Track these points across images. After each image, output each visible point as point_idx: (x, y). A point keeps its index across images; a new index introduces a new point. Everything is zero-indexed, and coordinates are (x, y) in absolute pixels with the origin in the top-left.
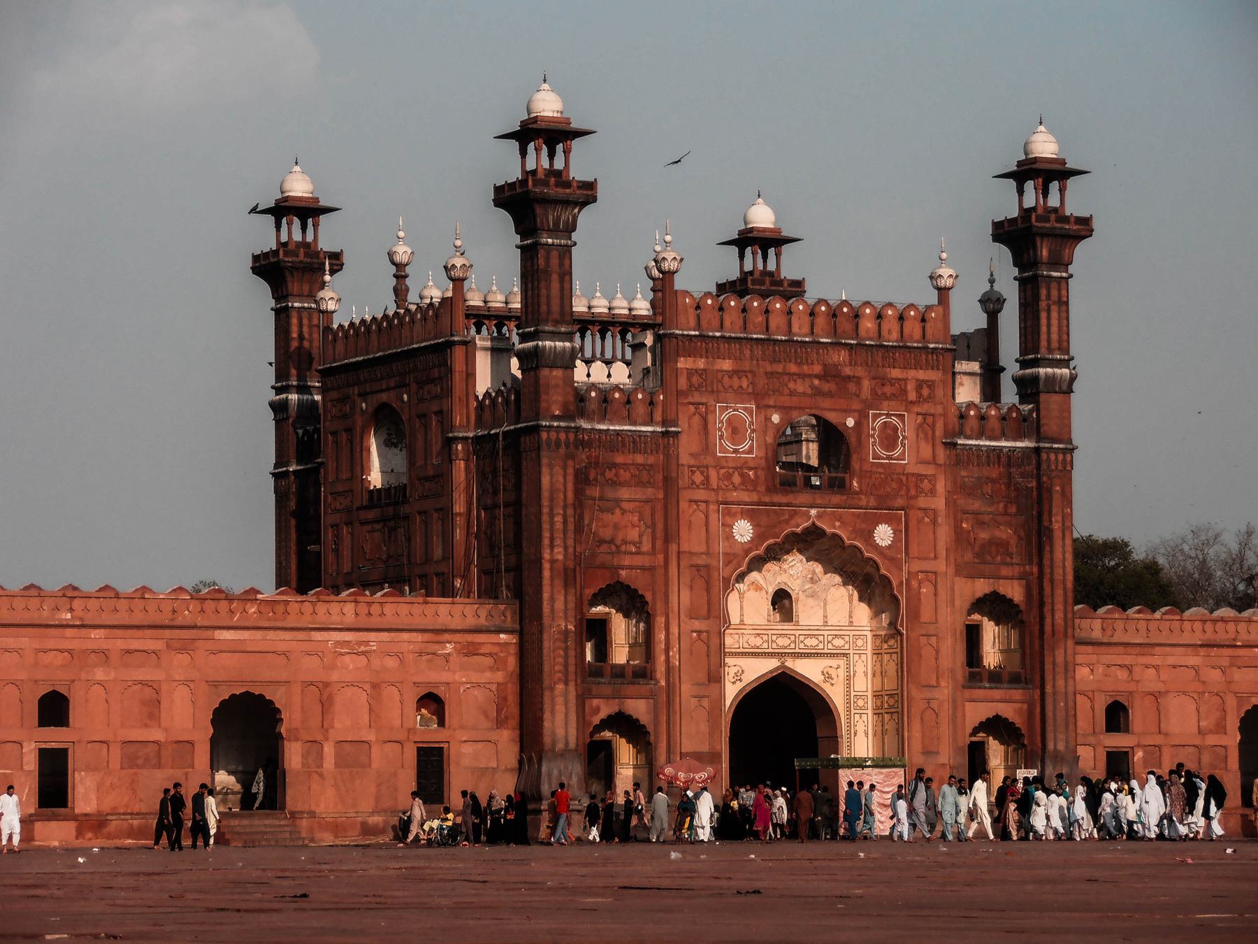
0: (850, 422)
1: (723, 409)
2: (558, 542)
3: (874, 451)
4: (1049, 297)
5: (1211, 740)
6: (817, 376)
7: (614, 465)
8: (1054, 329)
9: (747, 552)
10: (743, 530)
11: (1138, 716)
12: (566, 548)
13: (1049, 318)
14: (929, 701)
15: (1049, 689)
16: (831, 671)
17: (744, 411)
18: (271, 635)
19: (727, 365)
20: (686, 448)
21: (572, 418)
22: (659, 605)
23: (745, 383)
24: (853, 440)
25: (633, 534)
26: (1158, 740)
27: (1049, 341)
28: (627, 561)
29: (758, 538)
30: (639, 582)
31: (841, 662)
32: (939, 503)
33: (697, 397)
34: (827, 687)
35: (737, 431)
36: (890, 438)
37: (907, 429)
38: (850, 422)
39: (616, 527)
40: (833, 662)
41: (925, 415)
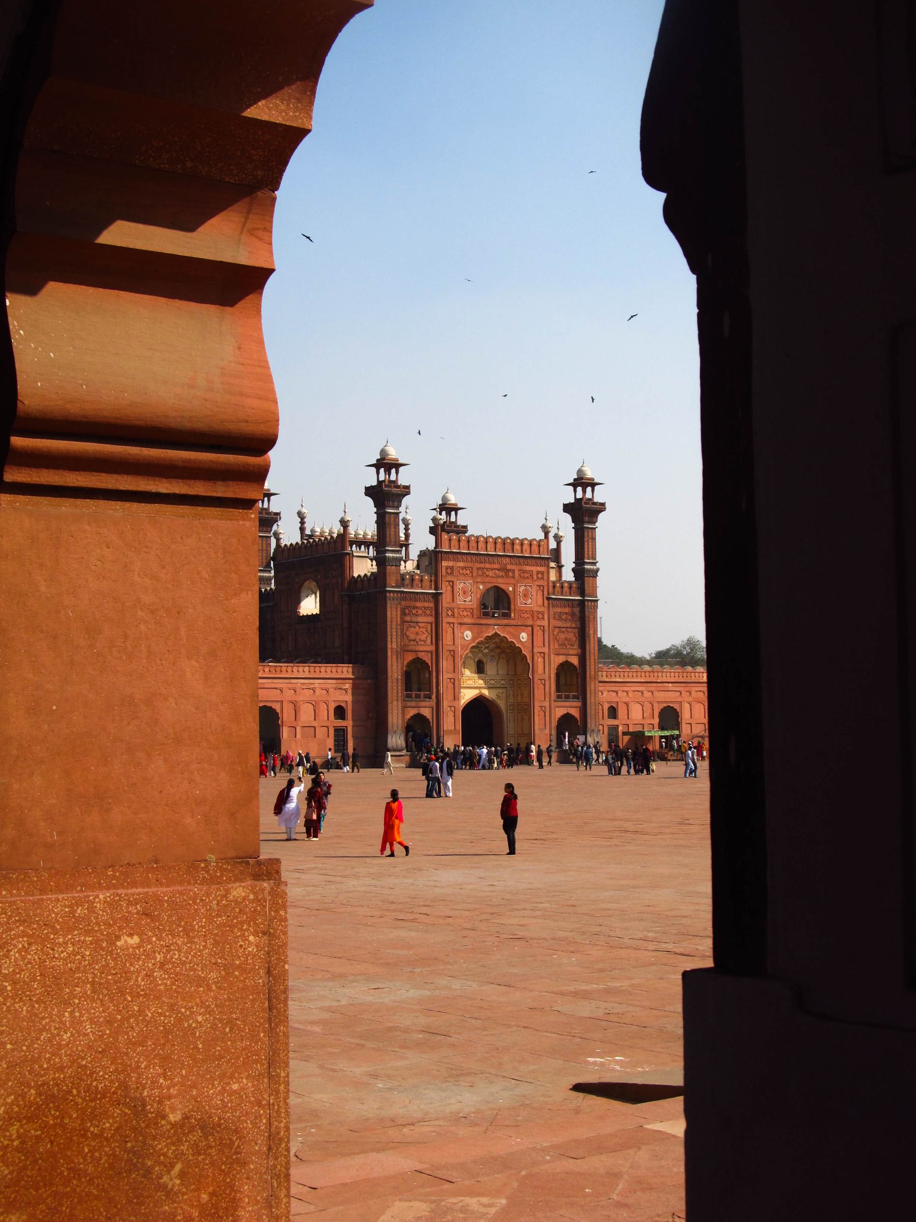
2: (394, 640)
3: (520, 603)
7: (417, 607)
10: (468, 635)
11: (622, 712)
18: (275, 681)
19: (461, 564)
20: (445, 601)
21: (399, 587)
23: (468, 572)
24: (511, 596)
25: (423, 637)
28: (421, 648)
29: (473, 639)
31: (504, 690)
32: (545, 623)
33: (449, 578)
34: (498, 701)
35: (464, 593)
37: (533, 590)
40: (500, 690)
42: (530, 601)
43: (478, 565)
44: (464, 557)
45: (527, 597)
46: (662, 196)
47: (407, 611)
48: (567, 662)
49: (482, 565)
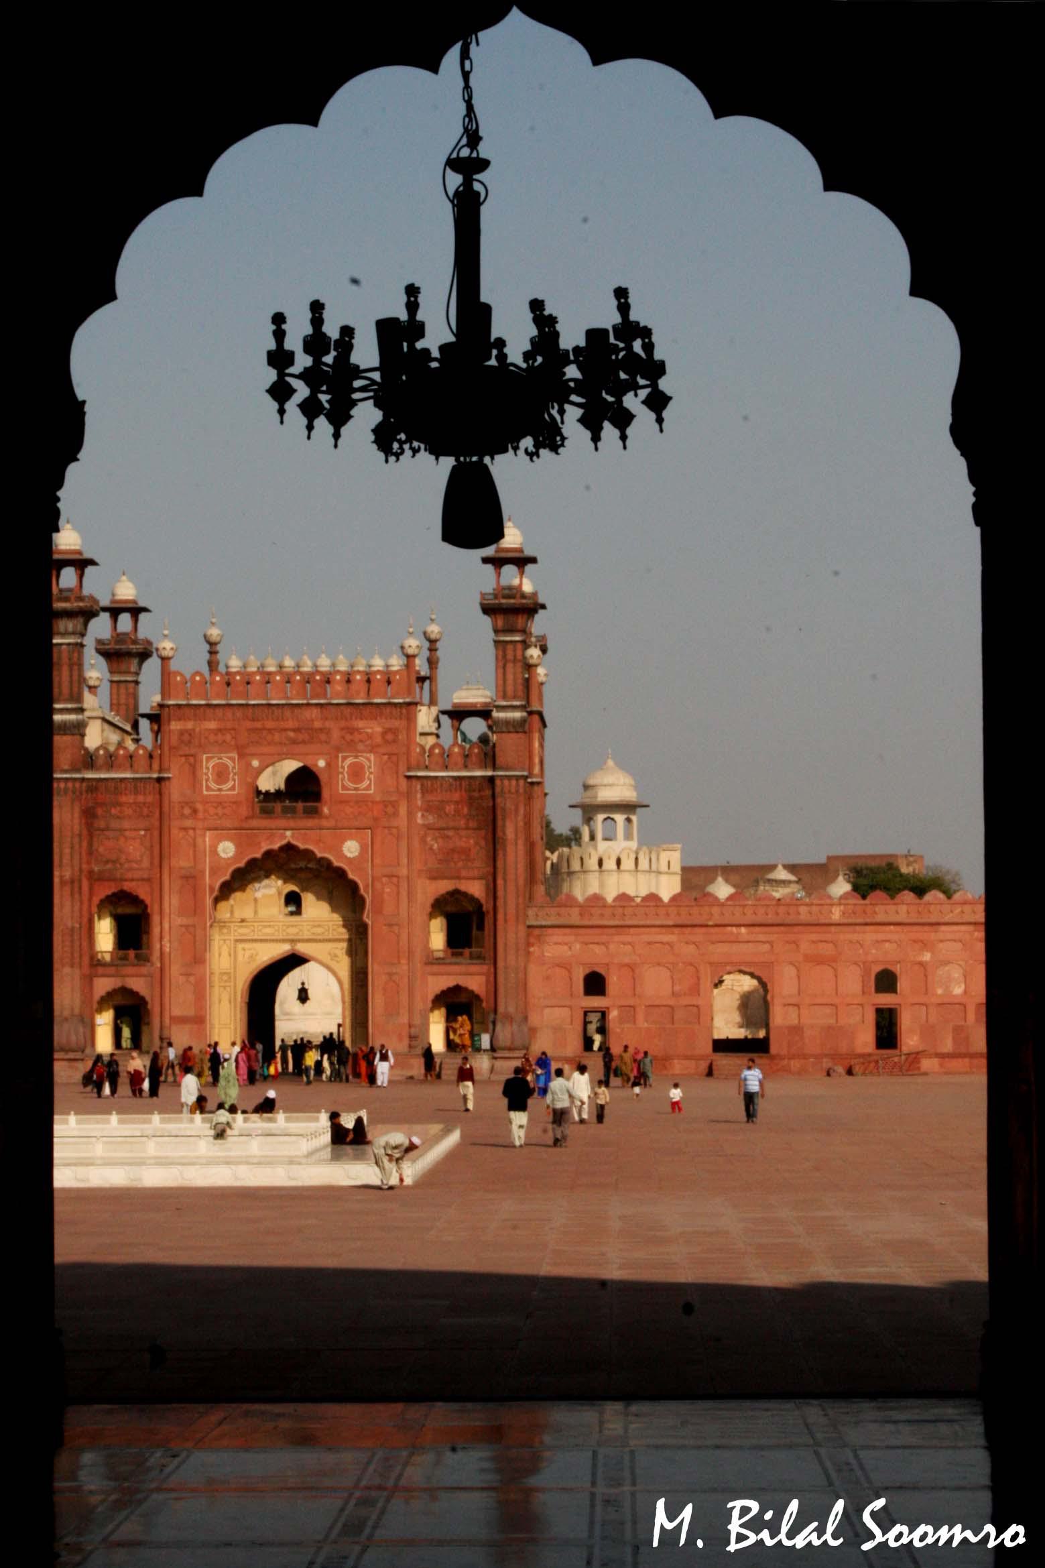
0: (322, 763)
1: (208, 759)
5: (686, 1001)
6: (294, 730)
7: (121, 805)
9: (229, 865)
10: (227, 849)
11: (614, 983)
12: (72, 866)
14: (390, 974)
17: (229, 760)
19: (212, 725)
20: (176, 791)
21: (78, 771)
22: (156, 907)
23: (228, 737)
24: (323, 778)
26: (631, 1002)
30: (142, 892)
33: (186, 750)
36: (357, 773)
38: (322, 763)
41: (390, 755)
42: (366, 783)
43: (249, 724)
44: (219, 712)
45: (356, 775)
46: (515, 14)
47: (99, 811)
48: (456, 892)
49: (258, 725)
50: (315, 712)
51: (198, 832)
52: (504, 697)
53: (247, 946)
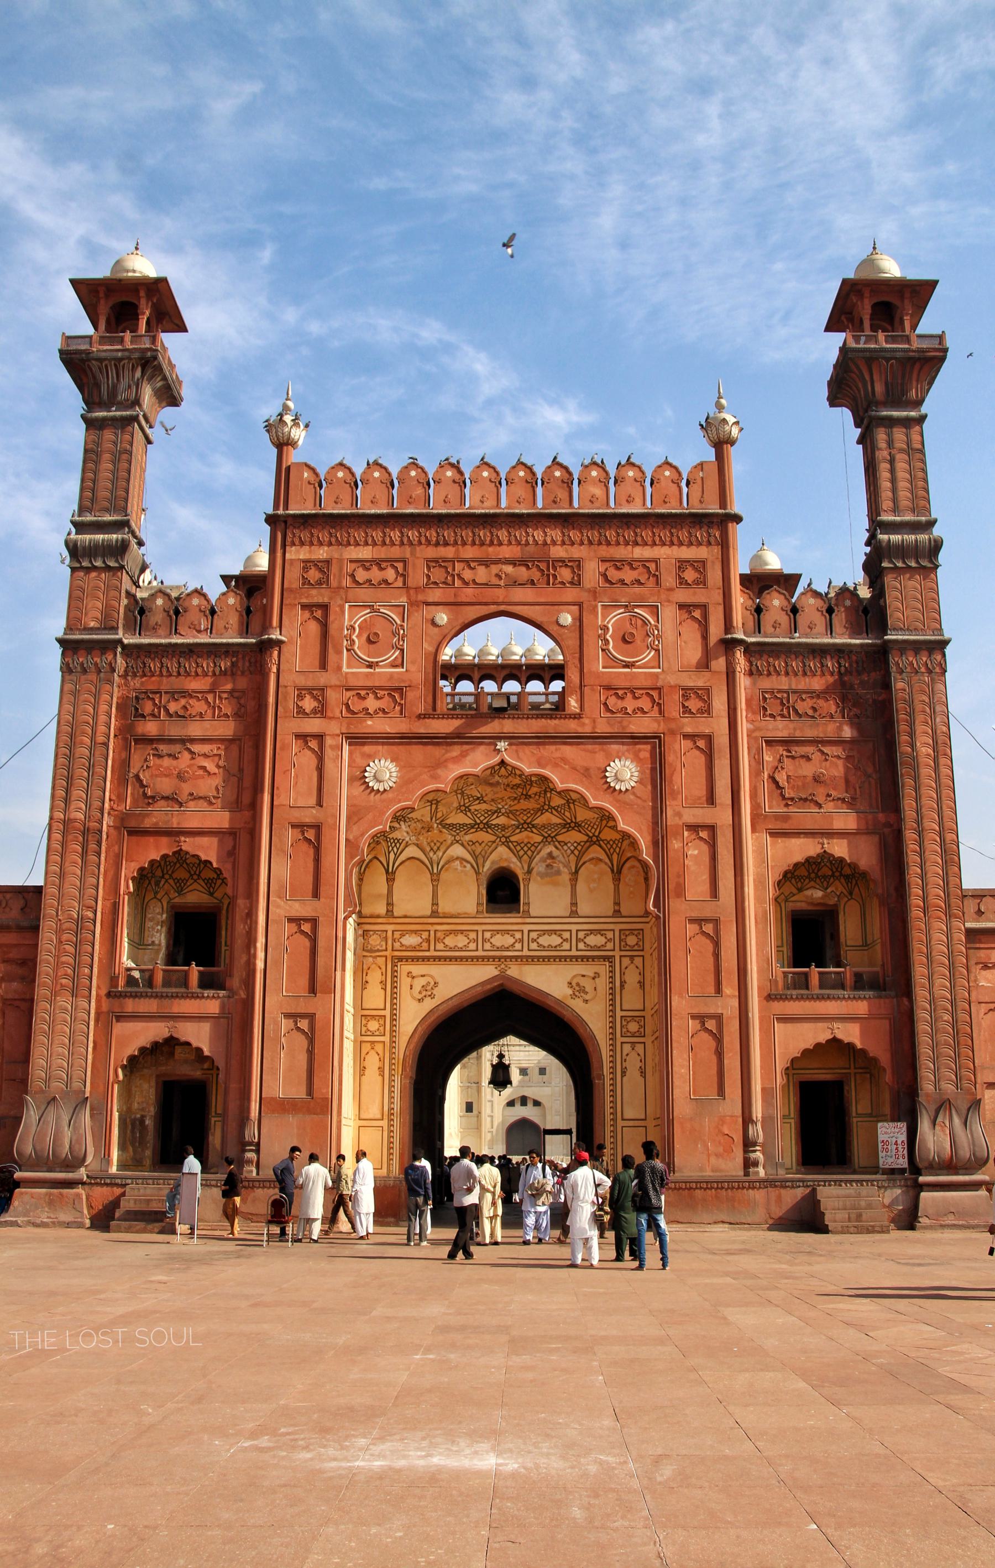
0: (567, 619)
4: (890, 443)
6: (513, 563)
7: (186, 694)
8: (903, 485)
13: (892, 471)
15: (921, 994)
16: (583, 982)
19: (365, 553)
23: (390, 574)
27: (895, 500)
29: (405, 783)
31: (603, 969)
34: (577, 1005)
39: (181, 777)
40: (588, 969)
43: (431, 552)
47: (148, 707)
49: (449, 552)
50: (555, 533)
51: (329, 741)
52: (896, 510)
53: (417, 969)
